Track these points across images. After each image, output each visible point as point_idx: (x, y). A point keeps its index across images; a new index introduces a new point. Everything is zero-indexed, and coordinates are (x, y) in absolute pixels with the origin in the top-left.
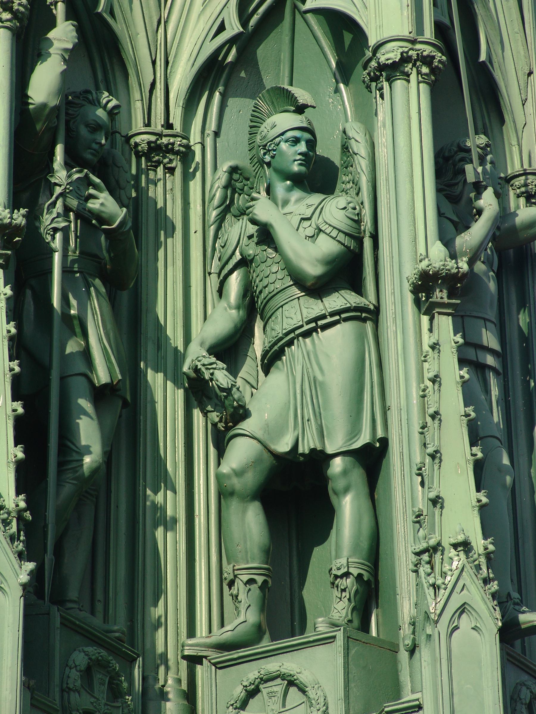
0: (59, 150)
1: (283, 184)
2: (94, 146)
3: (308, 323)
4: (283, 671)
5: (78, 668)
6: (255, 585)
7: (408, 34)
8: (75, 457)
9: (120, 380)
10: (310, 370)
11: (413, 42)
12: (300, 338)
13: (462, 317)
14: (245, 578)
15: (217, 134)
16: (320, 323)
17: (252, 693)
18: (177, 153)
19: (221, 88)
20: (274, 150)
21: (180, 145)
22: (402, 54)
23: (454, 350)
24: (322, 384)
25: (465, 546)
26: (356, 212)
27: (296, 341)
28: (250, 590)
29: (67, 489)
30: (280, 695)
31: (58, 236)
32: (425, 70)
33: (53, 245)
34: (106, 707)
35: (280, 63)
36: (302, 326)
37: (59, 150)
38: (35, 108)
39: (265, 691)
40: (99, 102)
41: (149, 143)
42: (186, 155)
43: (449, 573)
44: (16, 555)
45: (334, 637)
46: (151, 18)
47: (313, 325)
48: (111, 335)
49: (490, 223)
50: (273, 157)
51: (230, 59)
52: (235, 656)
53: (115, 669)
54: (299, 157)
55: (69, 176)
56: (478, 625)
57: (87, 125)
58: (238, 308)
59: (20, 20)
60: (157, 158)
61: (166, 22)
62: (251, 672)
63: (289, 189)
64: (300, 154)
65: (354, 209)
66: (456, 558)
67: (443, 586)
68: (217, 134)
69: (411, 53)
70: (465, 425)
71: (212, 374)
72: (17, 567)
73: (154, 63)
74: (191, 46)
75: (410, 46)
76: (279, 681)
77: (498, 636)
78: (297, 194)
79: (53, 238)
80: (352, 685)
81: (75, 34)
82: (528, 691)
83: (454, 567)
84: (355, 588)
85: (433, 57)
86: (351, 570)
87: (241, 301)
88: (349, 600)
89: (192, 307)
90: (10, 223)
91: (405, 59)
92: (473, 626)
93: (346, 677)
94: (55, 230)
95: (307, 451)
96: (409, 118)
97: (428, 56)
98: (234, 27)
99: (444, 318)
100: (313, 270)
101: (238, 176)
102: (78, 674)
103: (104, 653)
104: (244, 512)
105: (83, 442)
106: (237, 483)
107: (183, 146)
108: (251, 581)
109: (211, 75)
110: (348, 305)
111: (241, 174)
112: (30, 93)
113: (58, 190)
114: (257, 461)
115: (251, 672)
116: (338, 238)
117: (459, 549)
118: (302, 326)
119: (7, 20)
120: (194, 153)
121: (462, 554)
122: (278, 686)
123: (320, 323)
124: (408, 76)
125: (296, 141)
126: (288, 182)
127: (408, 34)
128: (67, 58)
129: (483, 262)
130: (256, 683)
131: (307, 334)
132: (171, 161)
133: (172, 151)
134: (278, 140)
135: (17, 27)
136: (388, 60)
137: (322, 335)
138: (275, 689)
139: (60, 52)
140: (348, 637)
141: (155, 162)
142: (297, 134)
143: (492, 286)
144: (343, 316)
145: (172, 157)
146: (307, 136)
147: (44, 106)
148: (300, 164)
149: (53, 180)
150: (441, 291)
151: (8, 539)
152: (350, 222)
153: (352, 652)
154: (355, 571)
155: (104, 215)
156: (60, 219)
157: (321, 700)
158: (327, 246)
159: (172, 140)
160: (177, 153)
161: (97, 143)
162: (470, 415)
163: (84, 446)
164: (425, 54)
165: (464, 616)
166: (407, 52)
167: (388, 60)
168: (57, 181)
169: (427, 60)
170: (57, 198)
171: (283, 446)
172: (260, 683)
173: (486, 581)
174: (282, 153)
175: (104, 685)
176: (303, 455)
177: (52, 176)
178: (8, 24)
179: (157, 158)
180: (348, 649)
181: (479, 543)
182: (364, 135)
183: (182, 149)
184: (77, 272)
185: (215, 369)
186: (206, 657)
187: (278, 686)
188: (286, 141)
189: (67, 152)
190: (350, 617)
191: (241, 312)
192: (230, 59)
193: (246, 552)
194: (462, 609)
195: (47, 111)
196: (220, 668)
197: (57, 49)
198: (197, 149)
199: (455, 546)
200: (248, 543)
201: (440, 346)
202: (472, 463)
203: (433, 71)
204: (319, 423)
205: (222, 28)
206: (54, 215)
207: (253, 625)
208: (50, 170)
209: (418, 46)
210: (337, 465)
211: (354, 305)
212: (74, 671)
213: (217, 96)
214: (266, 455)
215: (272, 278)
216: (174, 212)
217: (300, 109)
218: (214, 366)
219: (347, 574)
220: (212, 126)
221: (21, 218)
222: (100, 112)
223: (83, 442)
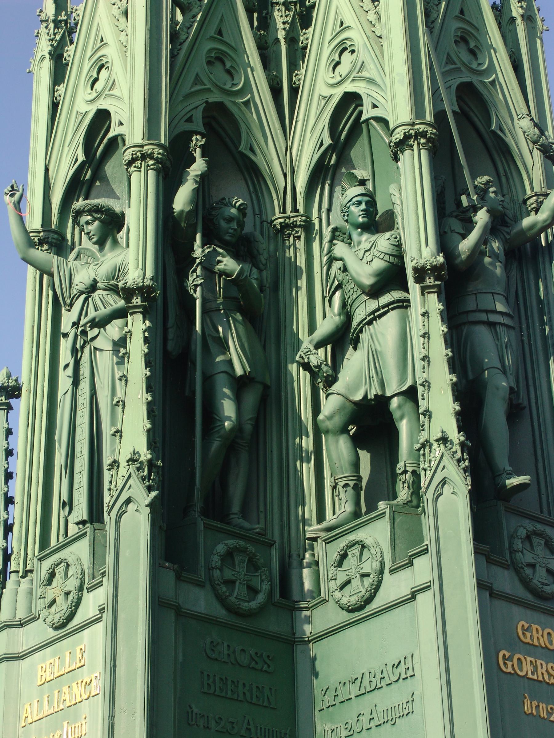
0: (198, 236)
1: (356, 232)
2: (231, 231)
3: (369, 315)
4: (358, 539)
5: (219, 554)
6: (349, 488)
7: (409, 120)
8: (219, 423)
9: (249, 372)
10: (373, 345)
11: (413, 124)
12: (366, 326)
13: (475, 294)
14: (342, 484)
15: (329, 210)
16: (376, 314)
17: (344, 556)
18: (300, 226)
19: (329, 182)
20: (347, 212)
21: (300, 221)
22: (405, 133)
23: (439, 315)
24: (381, 352)
25: (444, 440)
26: (397, 240)
27: (364, 329)
28: (346, 491)
29: (216, 444)
30: (358, 555)
31: (198, 289)
32: (423, 141)
33: (195, 295)
34: (246, 577)
35: (365, 158)
36: (366, 318)
37: (198, 236)
38: (177, 215)
40: (231, 204)
41: (281, 223)
42: (308, 227)
43: (433, 459)
44: (145, 488)
45: (385, 513)
46: (281, 148)
47: (372, 316)
48: (246, 345)
49: (481, 230)
50: (348, 216)
51: (332, 162)
52: (334, 534)
53: (251, 552)
54: (363, 212)
55: (203, 252)
56: (455, 491)
57: (224, 219)
58: (340, 315)
59: (161, 163)
60: (288, 232)
61: (291, 148)
62: (342, 543)
63: (361, 234)
64: (362, 211)
65: (396, 238)
66: (438, 449)
67: (429, 468)
68: (329, 210)
69: (410, 132)
70: (446, 362)
71: (308, 358)
72: (145, 495)
73: (285, 175)
74: (306, 159)
75: (410, 127)
76: (357, 546)
77: (468, 495)
78: (365, 237)
79: (195, 291)
80: (397, 542)
81: (205, 165)
82: (525, 530)
83: (437, 455)
84: (412, 479)
85: (427, 132)
86: (407, 469)
87: (341, 311)
88: (408, 487)
89: (312, 319)
90: (143, 285)
91: (407, 137)
92: (452, 492)
93: (393, 537)
94: (196, 286)
95: (373, 397)
96: (414, 173)
97: (423, 131)
98: (328, 141)
99: (431, 295)
100: (368, 281)
101: (339, 233)
102: (219, 557)
103: (242, 543)
104: (337, 442)
105: (226, 414)
106: (329, 425)
107: (303, 221)
108: (346, 486)
109: (321, 173)
110: (393, 299)
111: (340, 232)
112: (174, 206)
113: (198, 261)
114: (341, 409)
115: (342, 543)
116: (384, 259)
117: (440, 442)
118: (366, 318)
119: (152, 165)
120: (314, 224)
121: (442, 446)
123: (376, 314)
124: (412, 147)
125: (359, 203)
126: (359, 230)
127: (409, 120)
128: (198, 180)
129: (489, 257)
130: (345, 549)
131: (370, 323)
132: (297, 232)
133: (296, 226)
134: (348, 205)
135: (160, 168)
136: (396, 139)
137: (379, 321)
138: (355, 551)
139: (192, 178)
140: (394, 512)
141: (287, 234)
142: (359, 198)
143: (499, 271)
144: (390, 307)
145: (297, 229)
146: (366, 198)
147: (182, 212)
148: (363, 217)
149: (194, 256)
150: (430, 278)
151: (140, 479)
152: (392, 247)
153: (397, 521)
154: (410, 469)
155: (227, 271)
156: (198, 279)
157: (379, 555)
158: (379, 264)
159: (295, 219)
160: (300, 226)
161: (232, 229)
162: (448, 355)
163: (227, 416)
164: (420, 130)
165: (446, 486)
166: (408, 132)
167: (396, 139)
168: (196, 256)
169: (423, 134)
170: (197, 266)
171: (358, 397)
172: (347, 549)
173: (459, 461)
174: (352, 212)
175: (244, 563)
176: (371, 399)
177: (193, 254)
178: (153, 167)
179: (288, 232)
180: (394, 519)
181: (455, 436)
182: (398, 191)
183: (302, 223)
184: (222, 310)
185: (310, 355)
186: (319, 537)
187: (356, 550)
188: (353, 205)
189: (203, 236)
190: (409, 499)
191: (342, 317)
192: (332, 162)
193: (342, 467)
194: (444, 482)
195: (185, 214)
196: (328, 543)
197: (192, 176)
198: (316, 222)
199: (437, 440)
200: (342, 461)
201: (428, 314)
202: (450, 385)
203: (429, 140)
204: (380, 377)
205: (322, 144)
206: (195, 277)
207: (350, 513)
208: (193, 250)
209: (417, 127)
210: (395, 403)
211: (396, 299)
212: (216, 556)
213: (327, 187)
214: (348, 404)
215: (352, 291)
216: (301, 262)
217: (362, 183)
218: (309, 353)
219: (405, 472)
220: (325, 205)
221: (149, 281)
222: (233, 211)
223: (226, 414)
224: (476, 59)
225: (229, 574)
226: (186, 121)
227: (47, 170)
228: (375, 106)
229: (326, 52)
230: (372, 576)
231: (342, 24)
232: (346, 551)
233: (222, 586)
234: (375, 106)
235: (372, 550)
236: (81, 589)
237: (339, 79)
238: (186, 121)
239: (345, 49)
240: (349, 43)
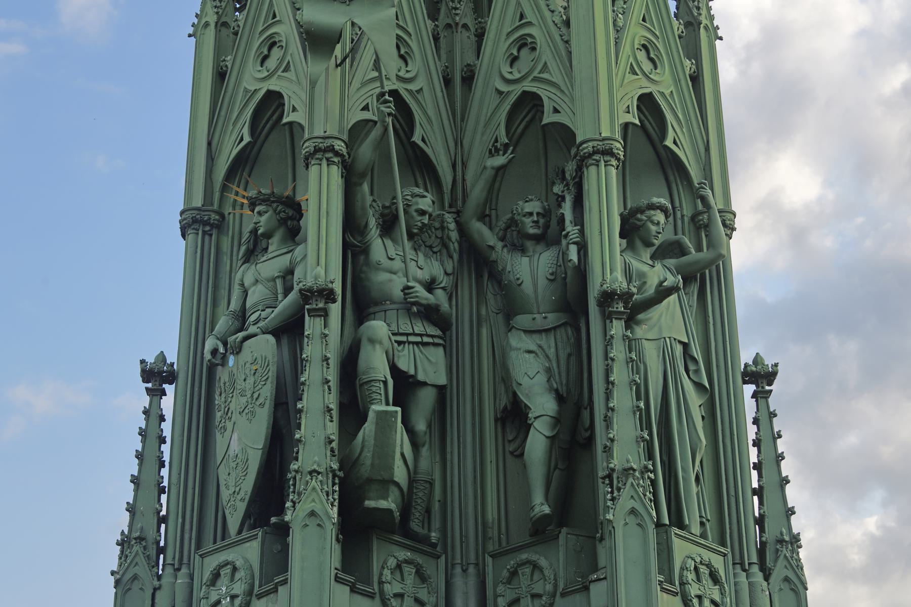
39: (520, 572)
122: (527, 570)
187: (527, 570)
224: (656, 68)
225: (397, 588)
226: (362, 109)
227: (209, 144)
228: (556, 111)
229: (504, 46)
230: (544, 598)
231: (522, 17)
232: (516, 569)
233: (392, 600)
234: (556, 111)
235: (546, 572)
236: (250, 593)
237: (517, 76)
238: (362, 109)
239: (525, 45)
240: (530, 40)
